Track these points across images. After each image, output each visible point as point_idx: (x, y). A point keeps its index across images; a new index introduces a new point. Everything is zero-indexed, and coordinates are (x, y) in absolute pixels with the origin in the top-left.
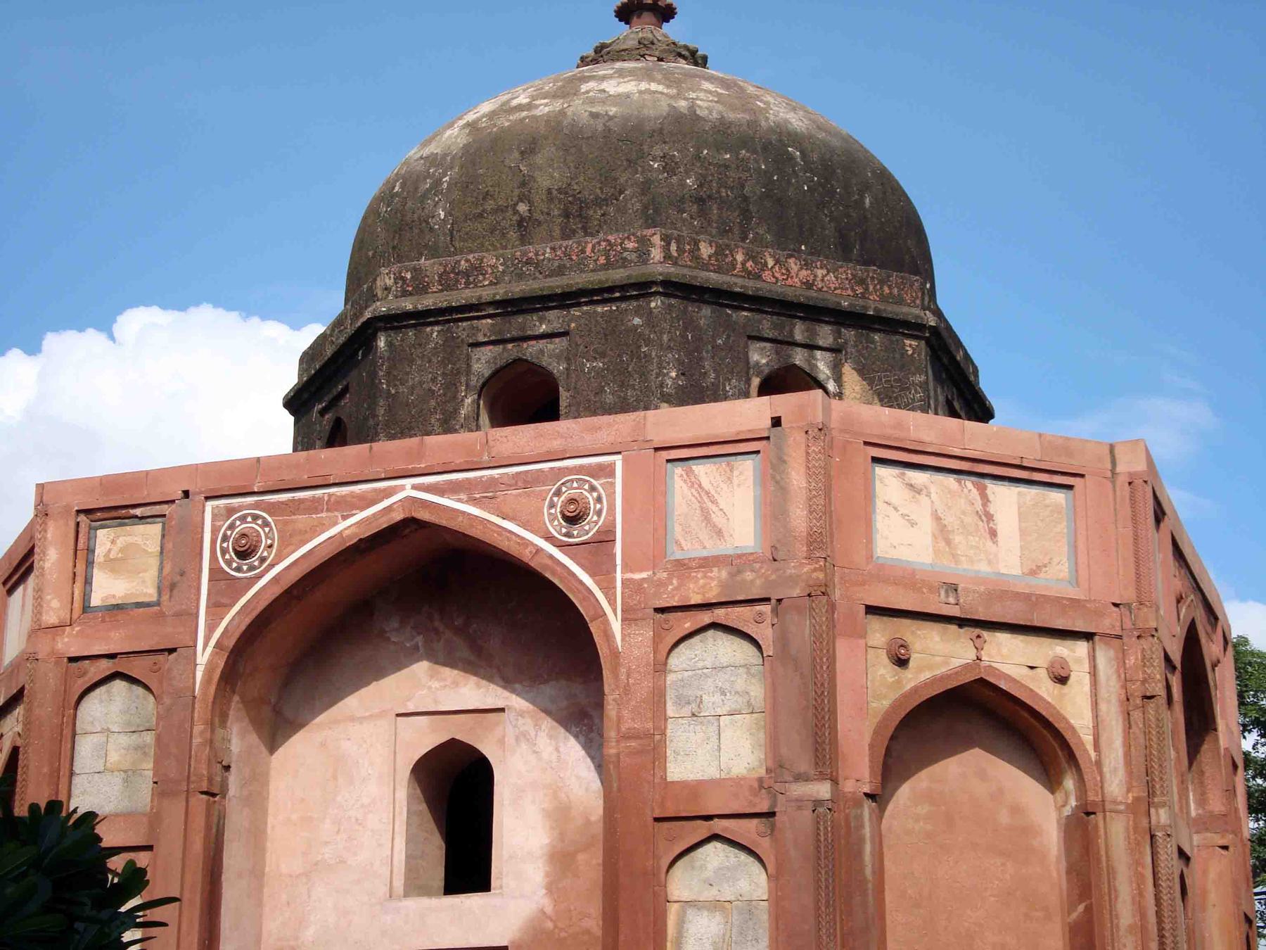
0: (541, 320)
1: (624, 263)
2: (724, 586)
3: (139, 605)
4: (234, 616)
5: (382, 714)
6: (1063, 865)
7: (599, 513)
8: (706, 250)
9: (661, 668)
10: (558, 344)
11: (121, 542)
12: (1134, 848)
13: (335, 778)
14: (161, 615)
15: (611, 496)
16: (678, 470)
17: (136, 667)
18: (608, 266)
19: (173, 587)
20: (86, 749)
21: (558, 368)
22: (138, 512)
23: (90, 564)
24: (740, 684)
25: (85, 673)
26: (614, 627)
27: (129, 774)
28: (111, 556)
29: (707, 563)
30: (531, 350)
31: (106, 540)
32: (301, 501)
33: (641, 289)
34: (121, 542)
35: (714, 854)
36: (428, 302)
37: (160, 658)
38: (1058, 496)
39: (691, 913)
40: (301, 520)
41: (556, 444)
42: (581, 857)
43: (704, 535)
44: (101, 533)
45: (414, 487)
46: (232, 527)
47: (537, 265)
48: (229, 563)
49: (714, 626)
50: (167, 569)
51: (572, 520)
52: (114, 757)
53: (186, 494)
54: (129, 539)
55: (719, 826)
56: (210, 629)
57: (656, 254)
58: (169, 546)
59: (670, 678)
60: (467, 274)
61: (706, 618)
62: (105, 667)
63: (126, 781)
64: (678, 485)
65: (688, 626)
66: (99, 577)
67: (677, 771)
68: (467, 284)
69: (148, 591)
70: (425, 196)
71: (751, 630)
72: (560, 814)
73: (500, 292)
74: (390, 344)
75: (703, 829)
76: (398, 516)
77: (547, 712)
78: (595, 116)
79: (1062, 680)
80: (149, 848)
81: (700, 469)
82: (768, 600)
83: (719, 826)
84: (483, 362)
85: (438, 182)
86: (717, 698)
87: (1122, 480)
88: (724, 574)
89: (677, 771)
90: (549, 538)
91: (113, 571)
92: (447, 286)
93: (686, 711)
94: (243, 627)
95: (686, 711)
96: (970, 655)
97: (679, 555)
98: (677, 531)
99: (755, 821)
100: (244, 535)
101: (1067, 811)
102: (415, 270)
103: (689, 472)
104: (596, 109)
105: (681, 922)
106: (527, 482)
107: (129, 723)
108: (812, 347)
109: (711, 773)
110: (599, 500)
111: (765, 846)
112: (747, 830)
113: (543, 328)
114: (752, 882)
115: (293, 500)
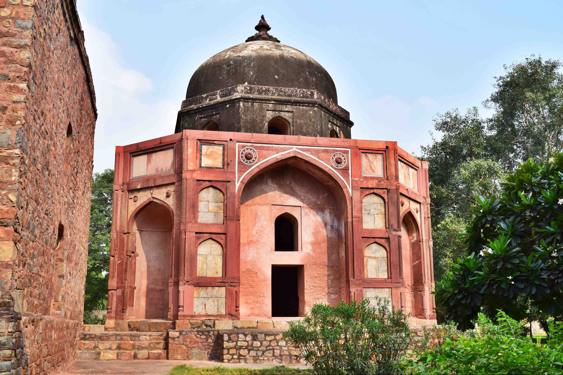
0: (286, 107)
1: (307, 97)
2: (377, 184)
3: (217, 168)
4: (246, 175)
5: (268, 204)
6: (411, 252)
7: (345, 162)
8: (323, 98)
9: (361, 202)
10: (290, 115)
11: (210, 150)
12: (426, 249)
13: (255, 219)
14: (225, 171)
15: (348, 158)
16: (363, 155)
17: (218, 185)
18: (303, 97)
19: (228, 164)
20: (202, 206)
21: (290, 120)
22: (216, 142)
23: (201, 155)
24: (379, 208)
25: (202, 185)
26: (349, 190)
27: (216, 214)
28: (208, 153)
29: (373, 178)
30: (282, 114)
31: (205, 148)
32: (264, 147)
33: (313, 104)
34: (210, 150)
35: (374, 246)
36: (256, 95)
37: (225, 183)
38: (416, 172)
39: (369, 260)
40: (264, 152)
41: (335, 144)
42: (322, 244)
43: (370, 171)
44: (203, 146)
45: (296, 148)
46: (244, 151)
47: (285, 93)
48: (244, 160)
49: (374, 193)
50: (226, 159)
51: (338, 162)
52: (211, 208)
53: (231, 140)
54: (213, 150)
55: (377, 240)
56: (239, 178)
57: (315, 96)
58: (226, 153)
59: (363, 204)
60: (265, 91)
61: (372, 191)
62: (208, 184)
63: (215, 215)
64: (364, 160)
65: (368, 192)
66: (203, 158)
67: (365, 226)
68: (265, 94)
69: (220, 165)
70: (245, 67)
71: (383, 195)
72: (315, 233)
73: (276, 97)
74: (244, 105)
75: (373, 240)
76: (292, 155)
77: (312, 209)
78: (292, 57)
79: (417, 212)
80: (225, 234)
81: (369, 155)
82: (387, 189)
83: (377, 240)
84: (270, 115)
85: (249, 64)
86: (374, 210)
87: (424, 170)
88: (377, 181)
89: (365, 226)
90: (332, 167)
91: (208, 157)
92: (260, 93)
93: (367, 212)
94: (249, 178)
95: (367, 212)
96: (408, 207)
97: (364, 175)
98: (363, 169)
99: (384, 240)
100: (249, 154)
101: (413, 241)
102: (250, 87)
103: (366, 156)
104: (293, 56)
105: (367, 261)
106: (327, 151)
107: (215, 200)
108: (337, 125)
109: (373, 227)
110: (345, 159)
111: (386, 245)
112: (383, 241)
113: (287, 109)
114: (383, 253)
115: (262, 146)
